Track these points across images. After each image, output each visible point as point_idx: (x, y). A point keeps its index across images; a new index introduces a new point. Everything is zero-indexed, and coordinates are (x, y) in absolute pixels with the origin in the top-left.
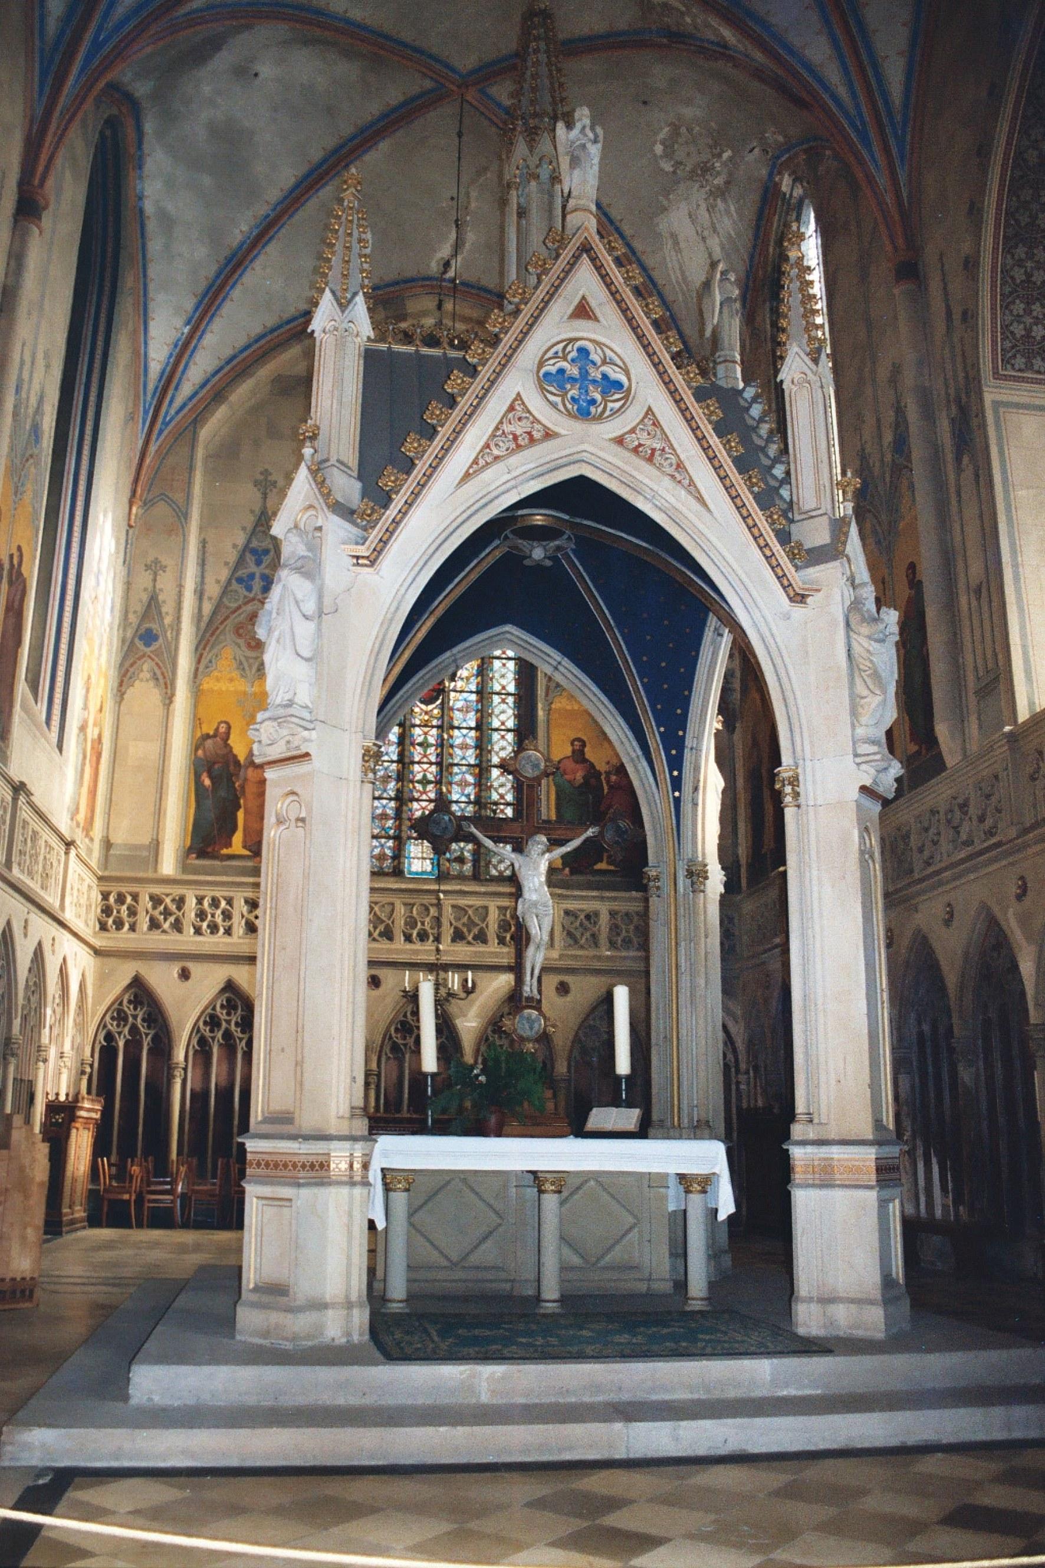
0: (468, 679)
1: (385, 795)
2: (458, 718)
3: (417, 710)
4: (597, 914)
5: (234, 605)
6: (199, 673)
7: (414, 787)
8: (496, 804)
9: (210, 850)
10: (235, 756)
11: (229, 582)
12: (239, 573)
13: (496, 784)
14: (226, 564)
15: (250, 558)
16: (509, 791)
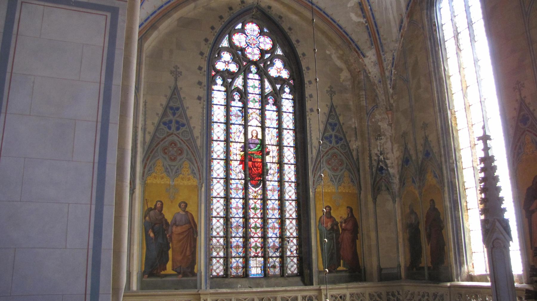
0: (273, 174)
1: (238, 235)
4: (345, 296)
5: (162, 137)
6: (145, 174)
8: (289, 238)
9: (155, 272)
10: (166, 220)
11: (159, 125)
12: (164, 120)
13: (288, 228)
14: (157, 114)
15: (169, 112)
16: (294, 231)
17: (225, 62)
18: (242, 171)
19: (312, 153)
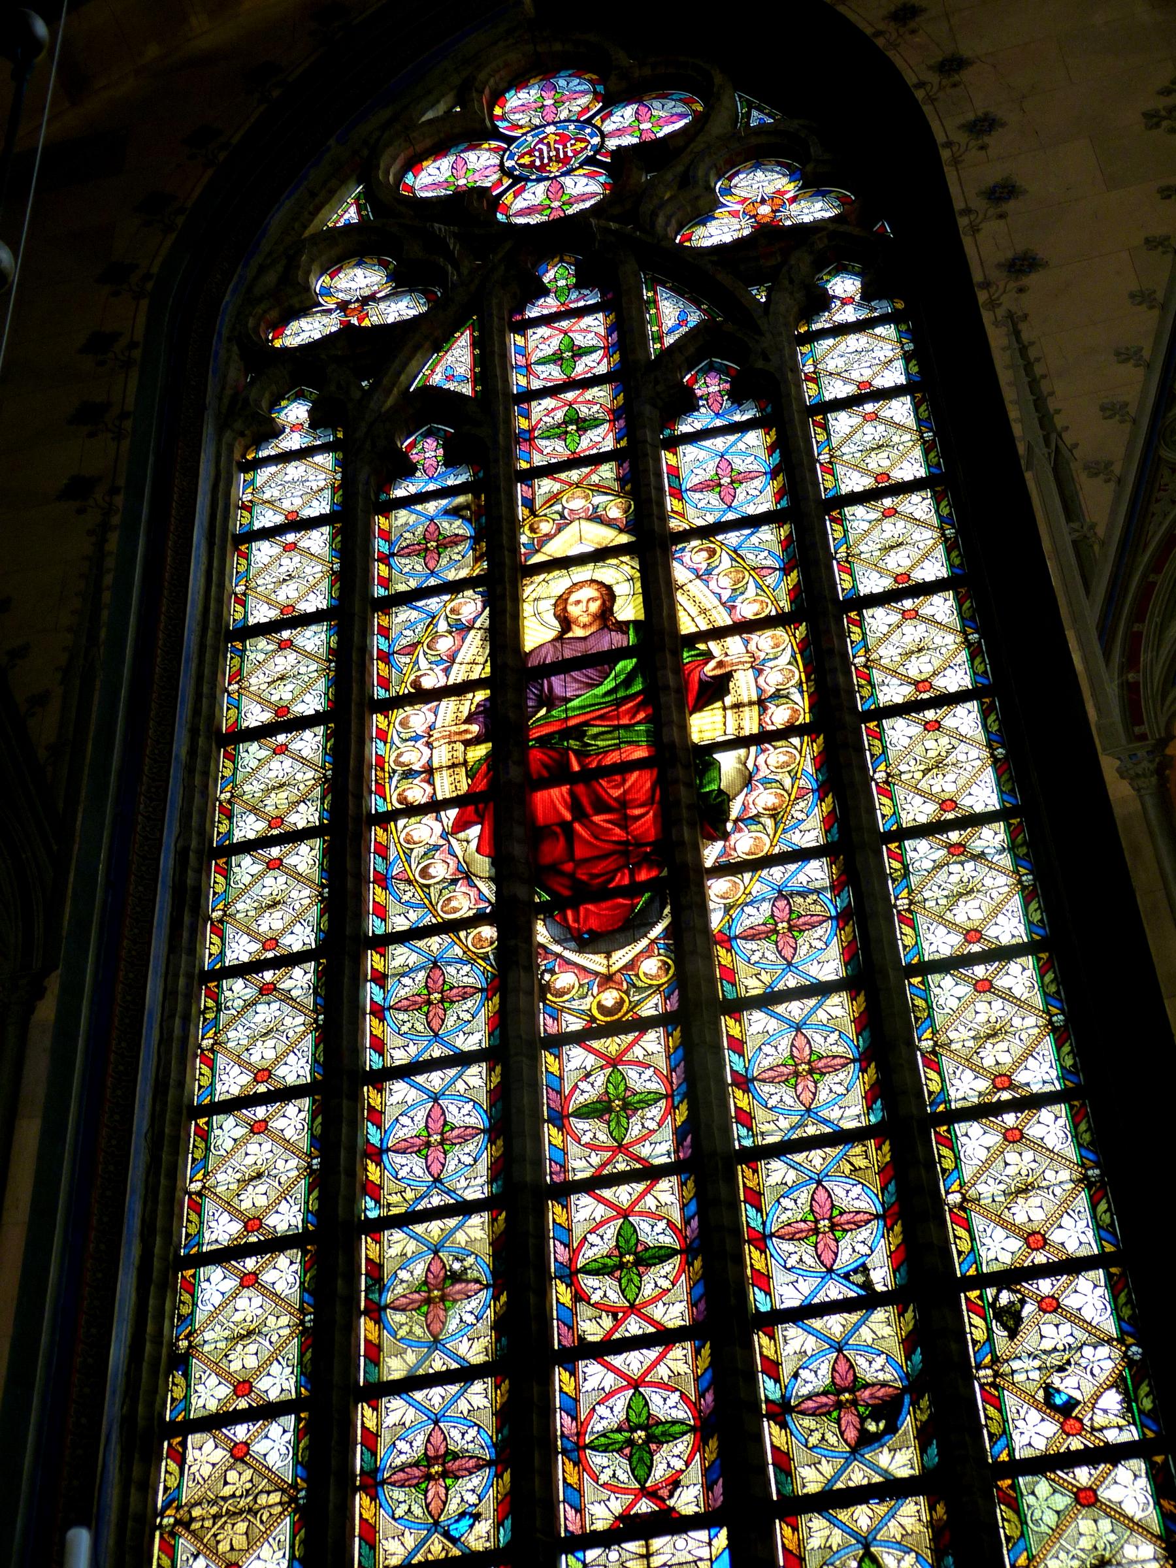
2: (751, 968)
3: (564, 979)
7: (580, 1296)
8: (1011, 1277)
16: (1065, 1208)
17: (343, 306)
18: (482, 865)
19: (1071, 509)
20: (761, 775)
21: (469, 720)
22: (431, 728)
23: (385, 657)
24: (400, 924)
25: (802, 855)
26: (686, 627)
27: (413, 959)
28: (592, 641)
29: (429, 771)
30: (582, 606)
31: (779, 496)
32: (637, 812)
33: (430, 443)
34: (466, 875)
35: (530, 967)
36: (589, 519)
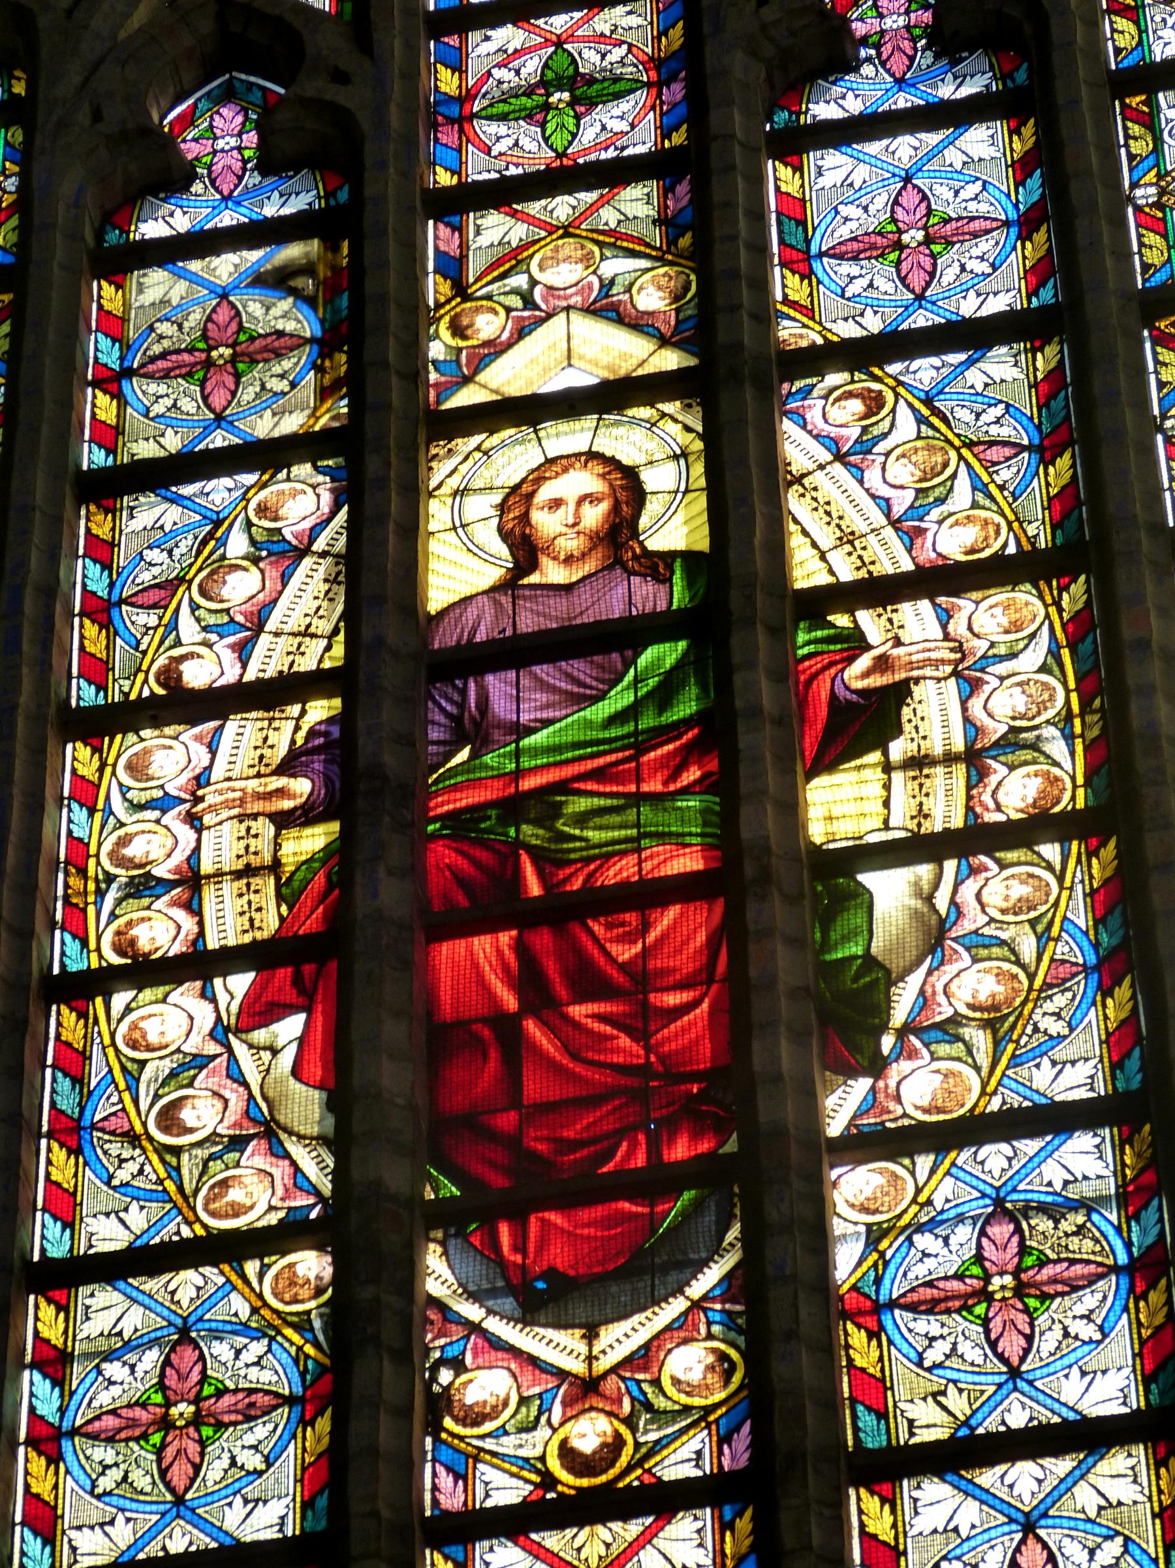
18: (305, 1106)
20: (967, 926)
21: (289, 766)
22: (201, 780)
23: (101, 611)
24: (107, 1235)
25: (1054, 1120)
26: (807, 572)
27: (134, 1320)
28: (584, 596)
29: (191, 883)
30: (566, 514)
31: (1037, 275)
32: (673, 999)
33: (229, 118)
34: (267, 1130)
35: (408, 1353)
36: (591, 311)
